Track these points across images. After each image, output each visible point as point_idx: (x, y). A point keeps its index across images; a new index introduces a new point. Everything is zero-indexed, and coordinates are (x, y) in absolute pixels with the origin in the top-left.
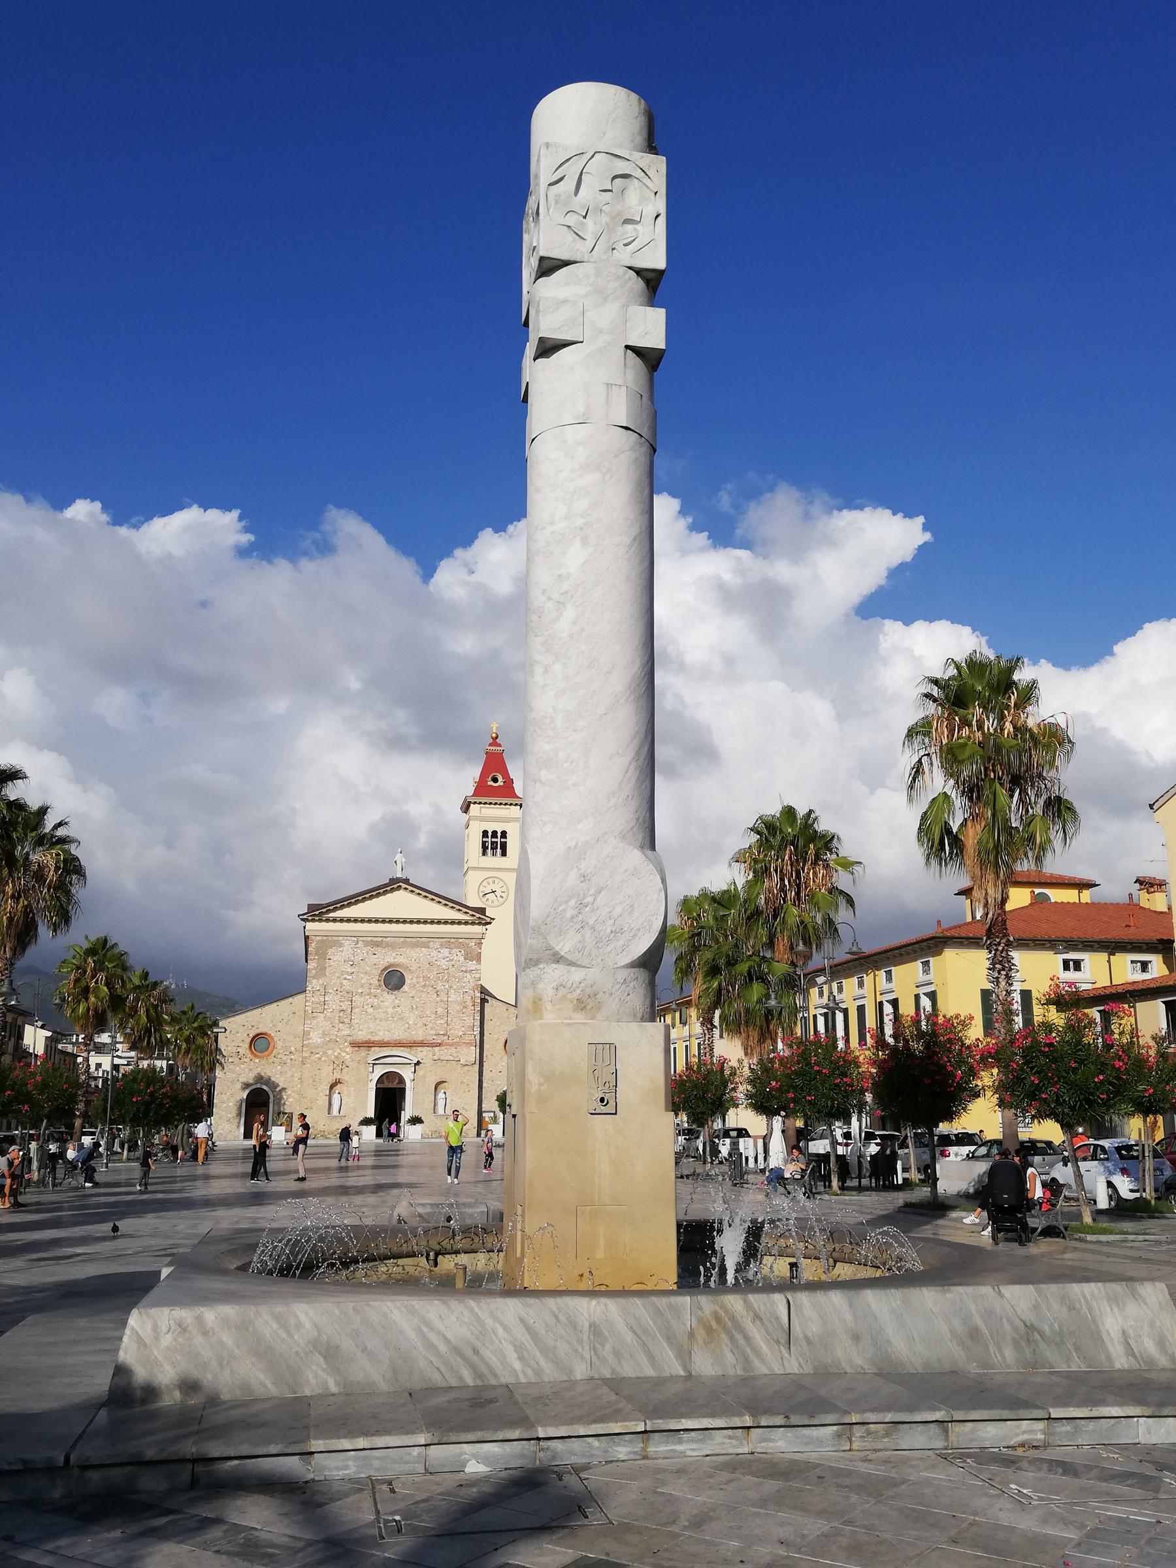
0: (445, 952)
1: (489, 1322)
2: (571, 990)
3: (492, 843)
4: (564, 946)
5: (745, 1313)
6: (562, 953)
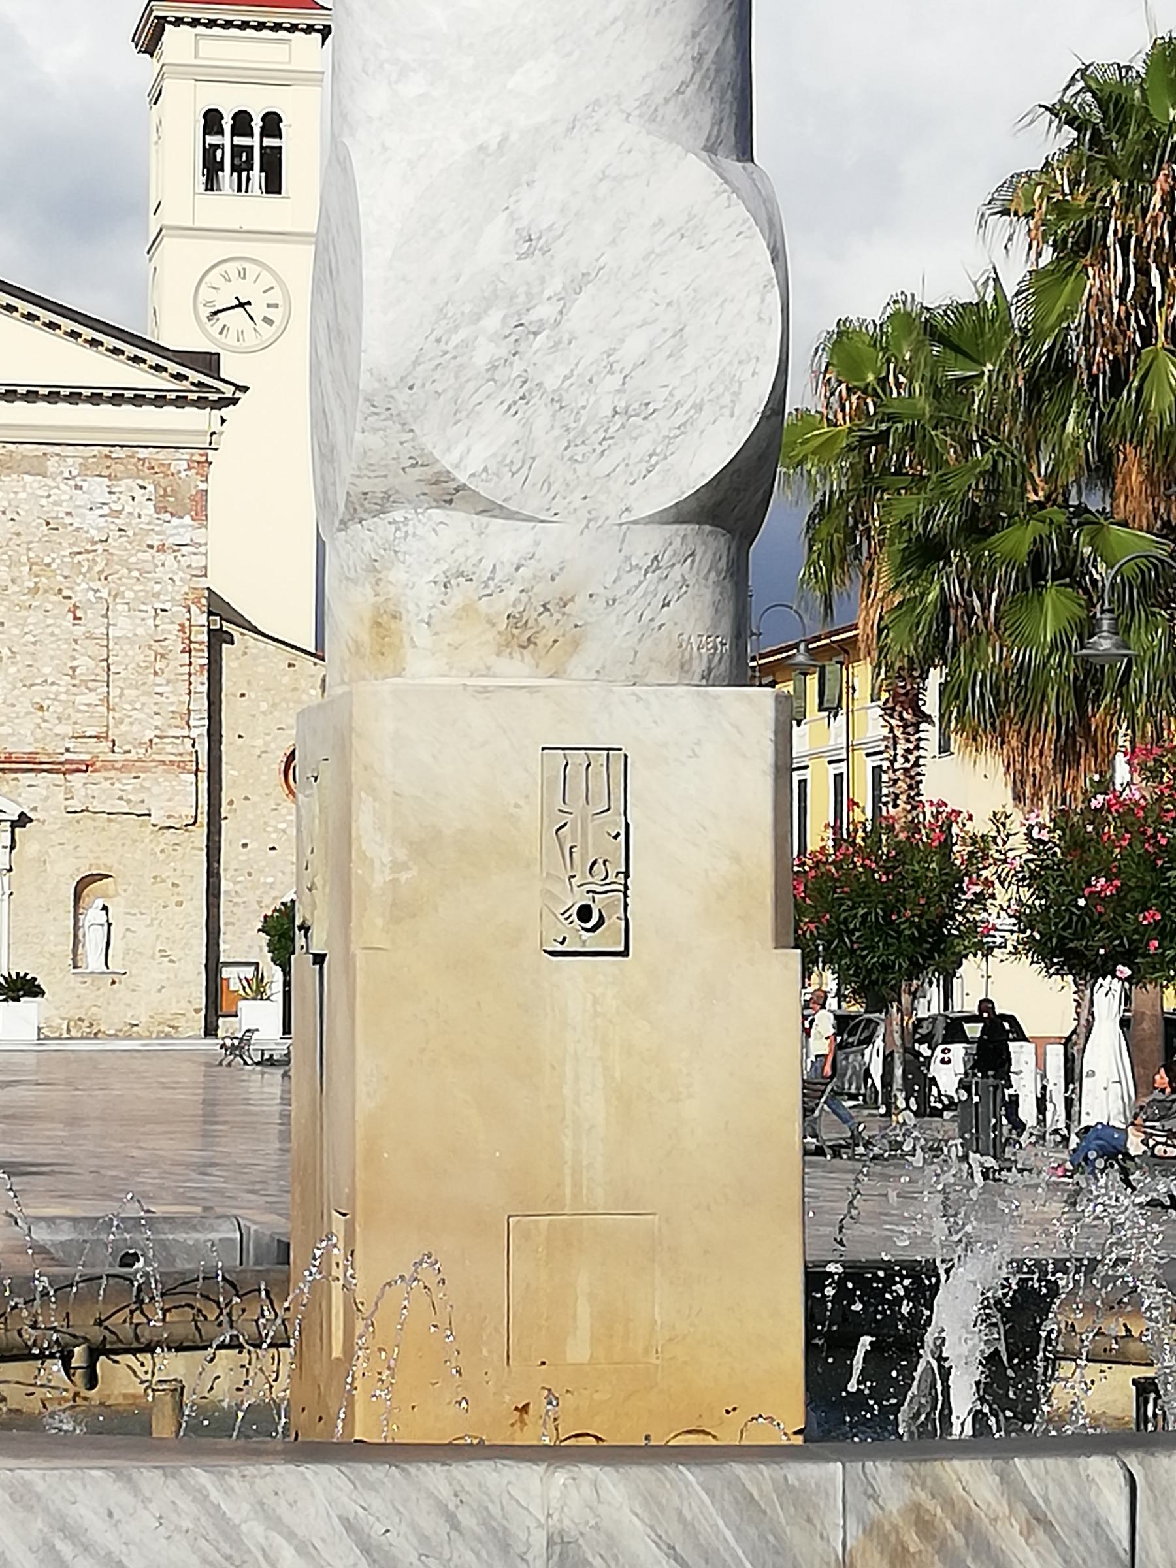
0: (97, 488)
1: (255, 1531)
2: (490, 587)
3: (236, 150)
4: (468, 456)
5: (1003, 1509)
6: (463, 478)
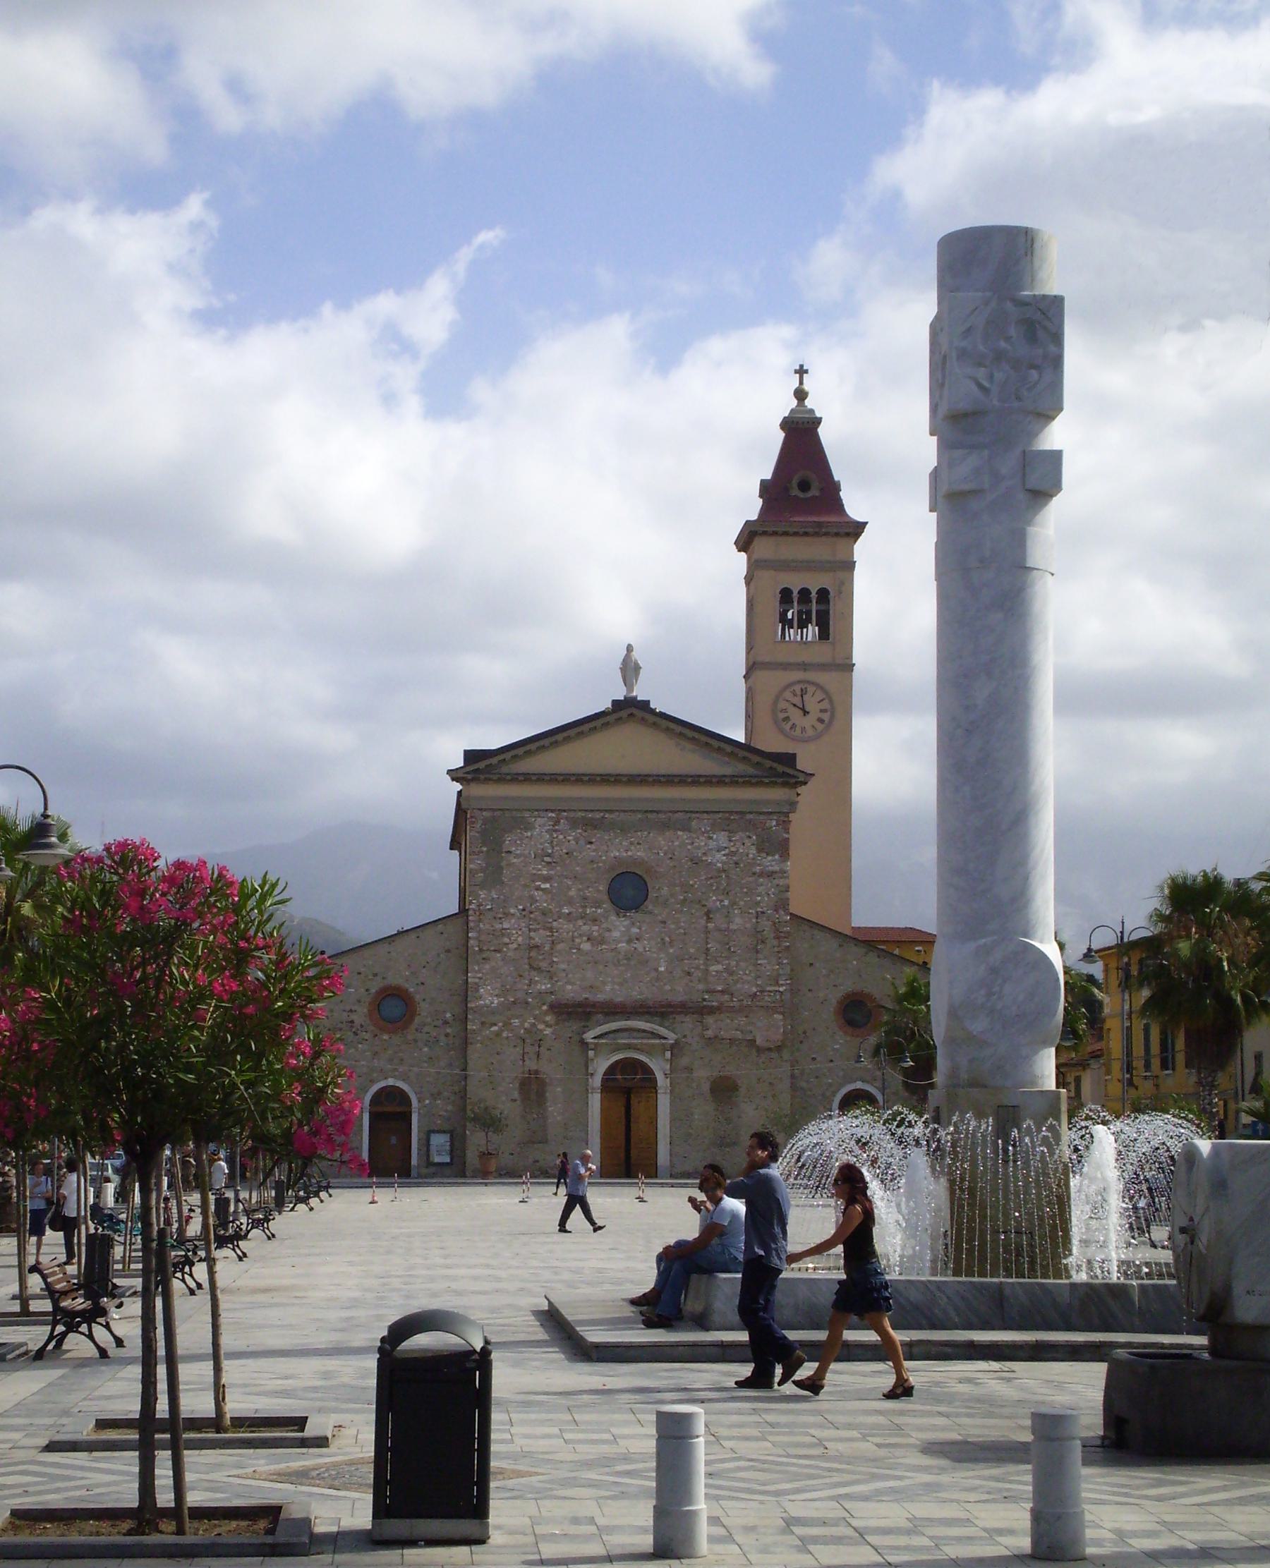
0: (721, 838)
